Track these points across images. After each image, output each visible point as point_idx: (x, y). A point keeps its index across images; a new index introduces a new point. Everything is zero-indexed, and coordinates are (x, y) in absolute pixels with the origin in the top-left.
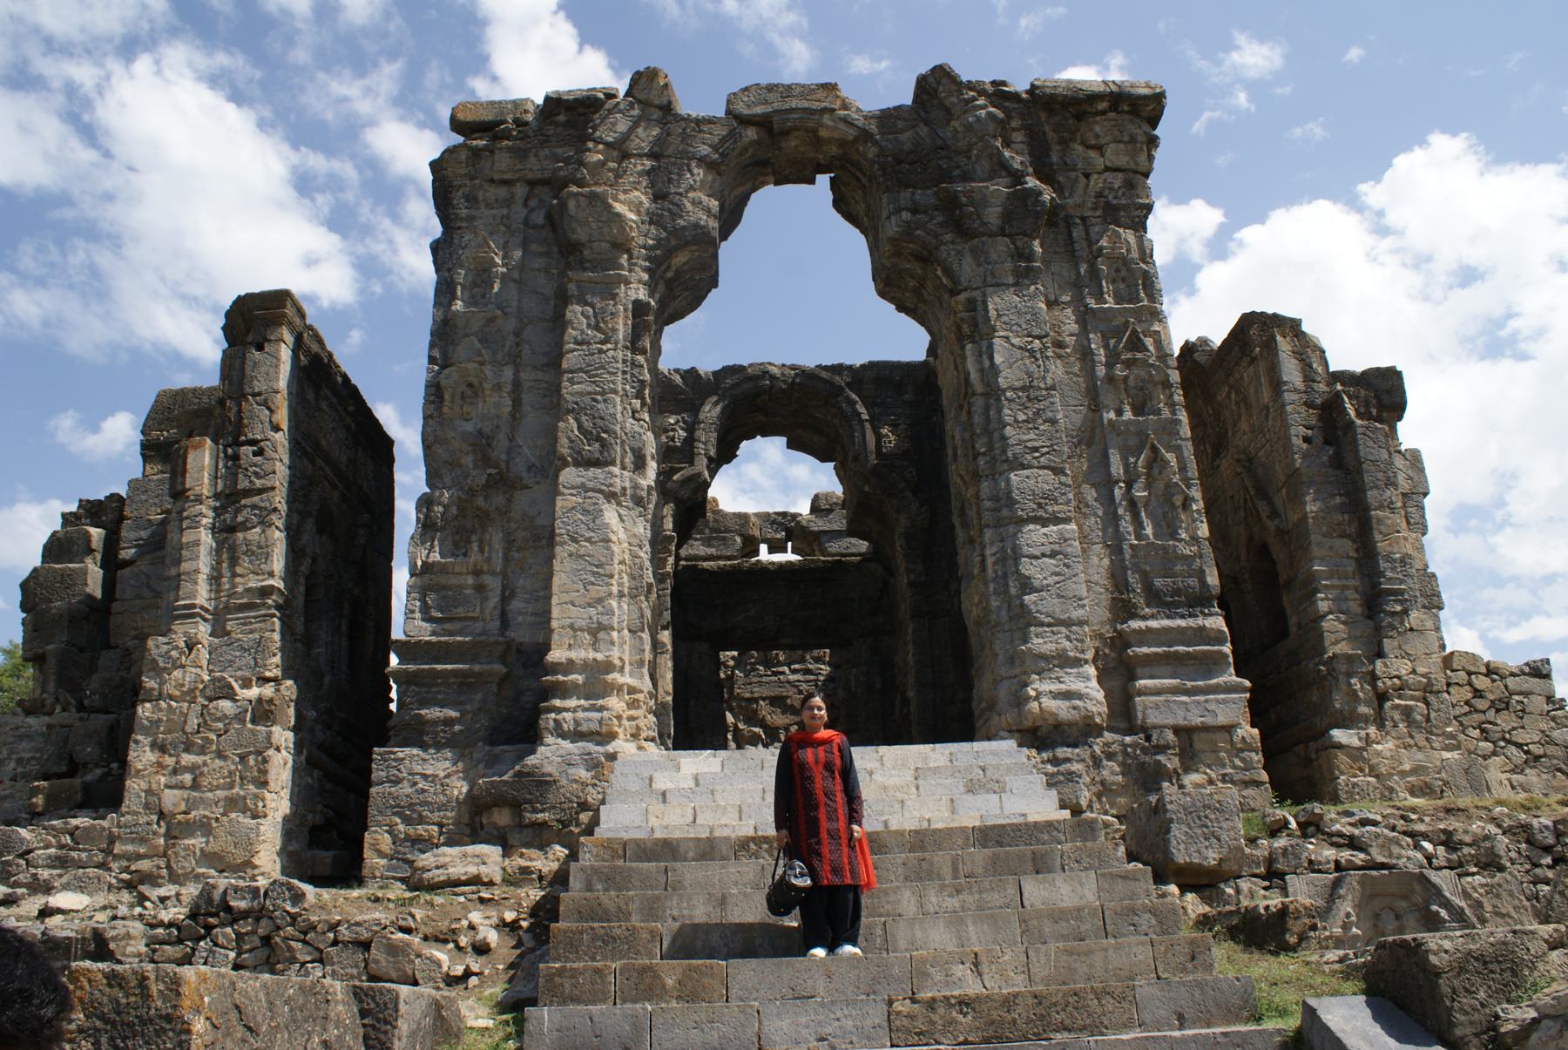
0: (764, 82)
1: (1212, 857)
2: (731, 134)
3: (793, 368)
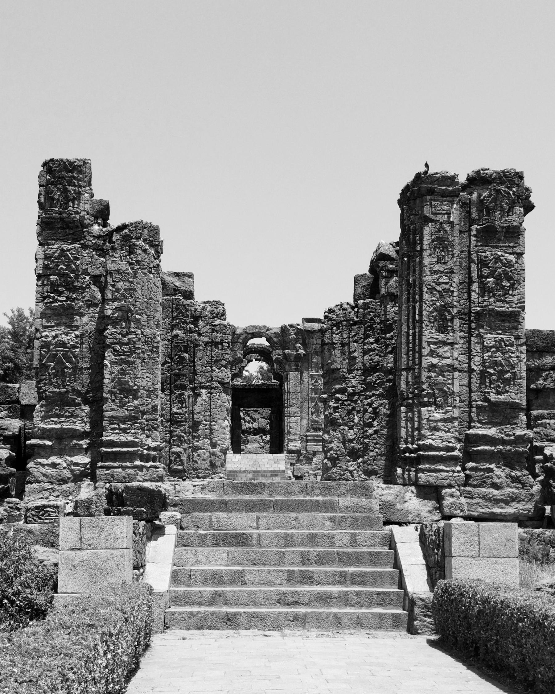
0: (252, 325)
1: (299, 475)
2: (246, 337)
3: (261, 345)
